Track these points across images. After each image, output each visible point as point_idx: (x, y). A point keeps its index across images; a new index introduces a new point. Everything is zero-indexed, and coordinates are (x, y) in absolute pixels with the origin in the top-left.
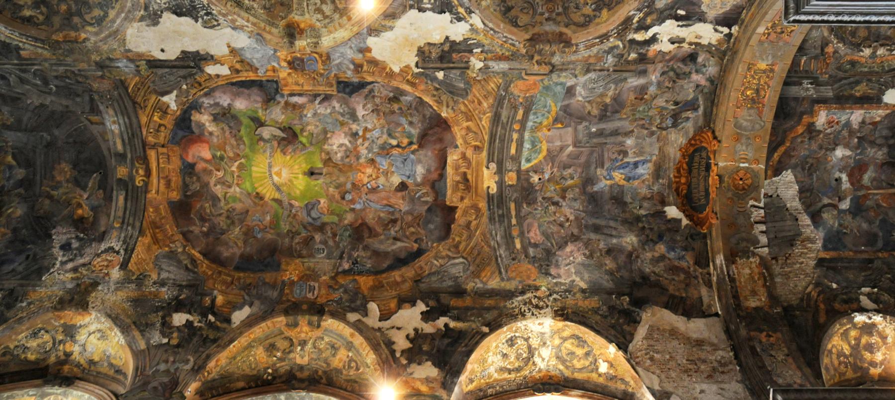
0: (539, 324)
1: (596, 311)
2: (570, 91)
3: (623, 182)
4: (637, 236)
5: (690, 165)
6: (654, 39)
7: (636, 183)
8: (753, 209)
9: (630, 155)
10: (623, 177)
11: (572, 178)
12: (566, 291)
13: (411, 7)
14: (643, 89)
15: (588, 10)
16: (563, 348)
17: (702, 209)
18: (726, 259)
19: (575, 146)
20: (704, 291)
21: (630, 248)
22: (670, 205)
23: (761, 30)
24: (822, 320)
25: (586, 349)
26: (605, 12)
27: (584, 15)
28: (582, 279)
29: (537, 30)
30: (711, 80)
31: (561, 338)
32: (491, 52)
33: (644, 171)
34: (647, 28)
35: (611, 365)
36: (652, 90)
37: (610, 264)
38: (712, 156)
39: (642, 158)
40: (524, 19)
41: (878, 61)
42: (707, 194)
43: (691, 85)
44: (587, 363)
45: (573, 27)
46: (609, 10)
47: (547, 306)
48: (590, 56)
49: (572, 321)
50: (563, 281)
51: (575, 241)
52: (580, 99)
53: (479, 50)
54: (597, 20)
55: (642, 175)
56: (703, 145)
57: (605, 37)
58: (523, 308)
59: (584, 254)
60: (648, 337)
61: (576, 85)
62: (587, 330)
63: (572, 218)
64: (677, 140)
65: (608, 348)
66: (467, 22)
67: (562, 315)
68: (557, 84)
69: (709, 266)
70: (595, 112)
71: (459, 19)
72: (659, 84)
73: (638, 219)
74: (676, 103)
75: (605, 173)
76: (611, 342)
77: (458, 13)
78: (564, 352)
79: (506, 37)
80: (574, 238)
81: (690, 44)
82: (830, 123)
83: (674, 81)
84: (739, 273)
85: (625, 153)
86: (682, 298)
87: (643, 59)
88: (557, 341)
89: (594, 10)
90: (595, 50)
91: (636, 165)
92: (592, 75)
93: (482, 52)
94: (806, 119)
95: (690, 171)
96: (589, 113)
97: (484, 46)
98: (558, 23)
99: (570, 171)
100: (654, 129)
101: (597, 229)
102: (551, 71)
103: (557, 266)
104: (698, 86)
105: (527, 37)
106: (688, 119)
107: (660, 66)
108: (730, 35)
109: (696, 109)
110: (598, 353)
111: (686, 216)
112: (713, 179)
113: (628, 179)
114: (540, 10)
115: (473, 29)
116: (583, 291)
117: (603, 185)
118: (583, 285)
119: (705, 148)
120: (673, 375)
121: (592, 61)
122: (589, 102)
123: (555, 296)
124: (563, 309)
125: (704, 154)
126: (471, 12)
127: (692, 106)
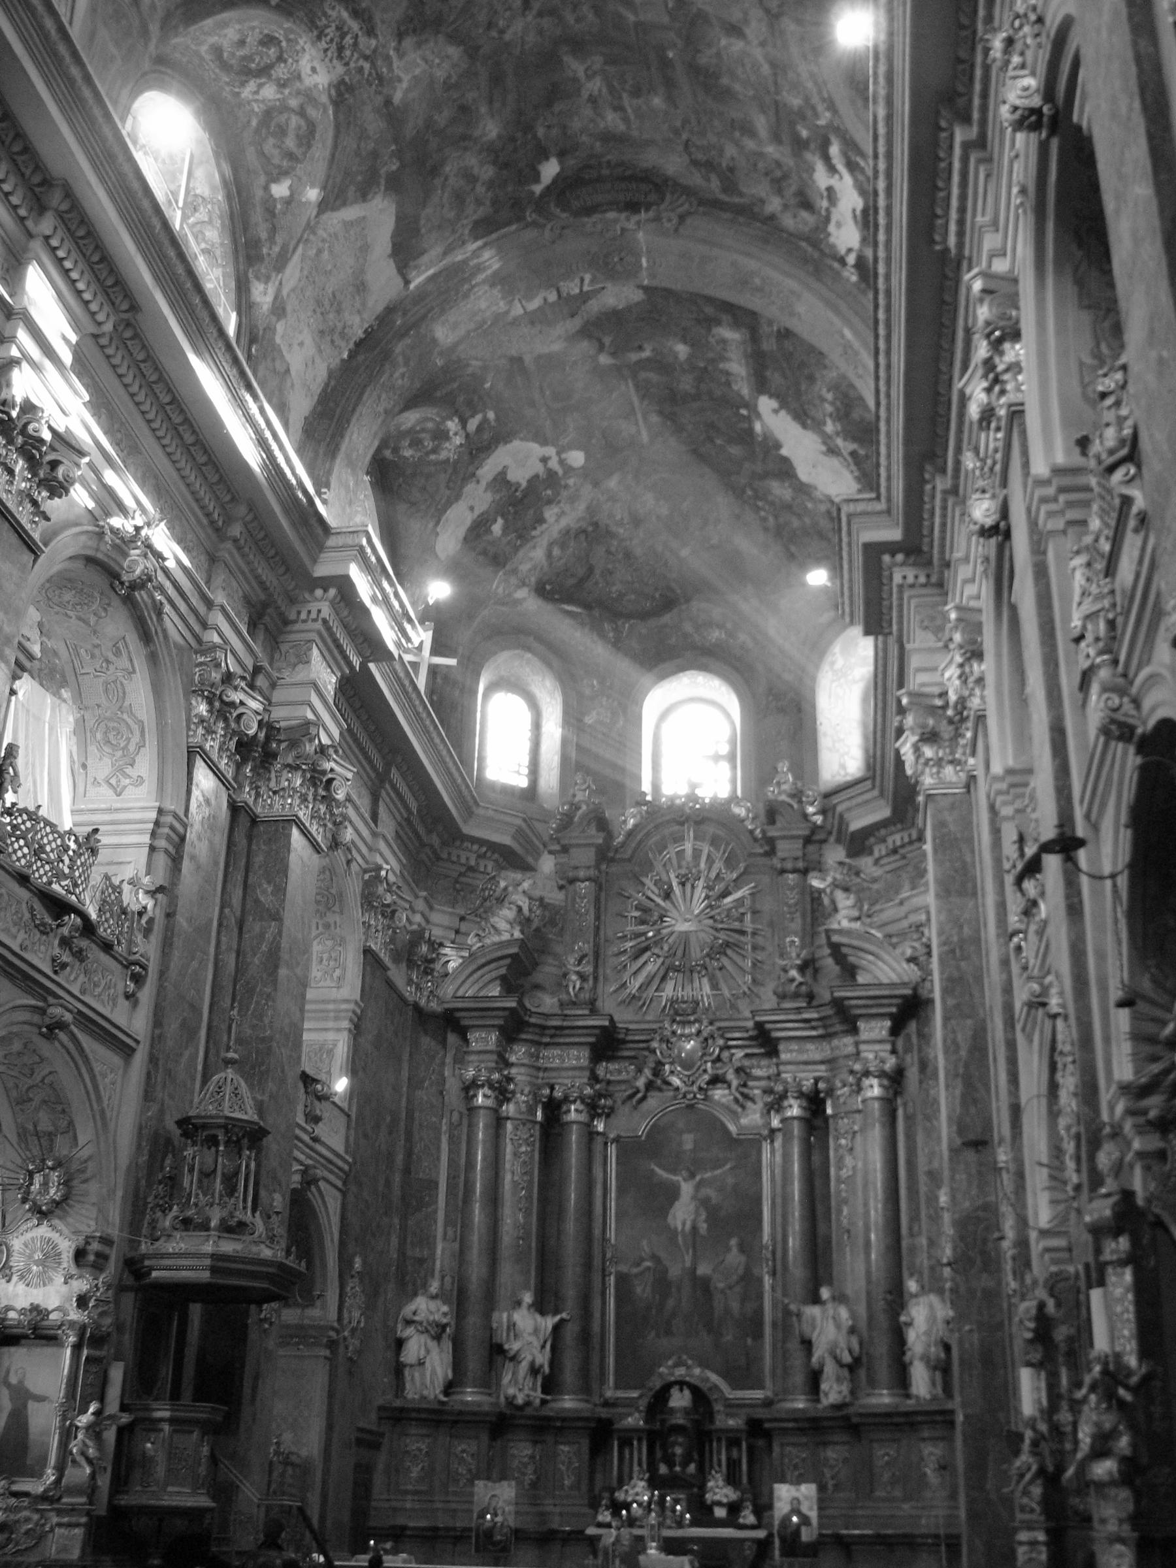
0: (314, 70)
1: (363, 136)
2: (735, 30)
3: (585, 94)
4: (499, 137)
5: (632, 178)
6: (832, 169)
7: (588, 112)
8: (577, 281)
9: (635, 101)
10: (596, 93)
11: (578, 20)
12: (380, 78)
14: (751, 132)
16: (286, 116)
17: (565, 206)
18: (495, 274)
19: (638, 24)
20: (438, 250)
21: (477, 133)
22: (561, 163)
23: (848, 333)
24: (438, 394)
25: (298, 152)
28: (408, 90)
30: (772, 217)
31: (302, 107)
33: (611, 120)
34: (852, 166)
35: (288, 201)
36: (750, 144)
37: (442, 118)
38: (651, 214)
39: (632, 117)
41: (817, 402)
42: (589, 211)
43: (763, 195)
44: (276, 161)
47: (347, 64)
48: (798, 75)
49: (336, 113)
50: (395, 66)
51: (471, 57)
52: (723, 42)
55: (603, 118)
56: (668, 197)
57: (832, 107)
58: (331, 31)
59: (449, 77)
60: (348, 225)
61: (748, 43)
62: (329, 142)
63: (507, 37)
64: (673, 164)
65: (312, 186)
67: (340, 94)
68: (746, 13)
69: (476, 239)
70: (703, 60)
72: (761, 155)
73: (528, 128)
74: (731, 170)
75: (597, 67)
76: (324, 188)
78: (283, 118)
80: (472, 52)
81: (828, 210)
82: (724, 341)
83: (767, 174)
84: (479, 298)
85: (636, 92)
86: (418, 230)
87: (800, 145)
88: (294, 103)
90: (810, 85)
91: (619, 108)
92: (766, 69)
94: (726, 318)
95: (623, 179)
96: (699, 51)
99: (591, 16)
100: (685, 136)
101: (497, 79)
102: (767, 11)
103: (419, 45)
104: (762, 201)
106: (708, 180)
107: (789, 162)
108: (842, 261)
109: (725, 190)
110: (298, 172)
111: (548, 188)
112: (616, 221)
113: (593, 100)
116: (388, 102)
117: (575, 67)
118: (398, 97)
119: (663, 200)
120: (308, 294)
121: (791, 75)
122: (718, 55)
123: (367, 66)
124: (350, 89)
125: (653, 197)
127: (730, 186)
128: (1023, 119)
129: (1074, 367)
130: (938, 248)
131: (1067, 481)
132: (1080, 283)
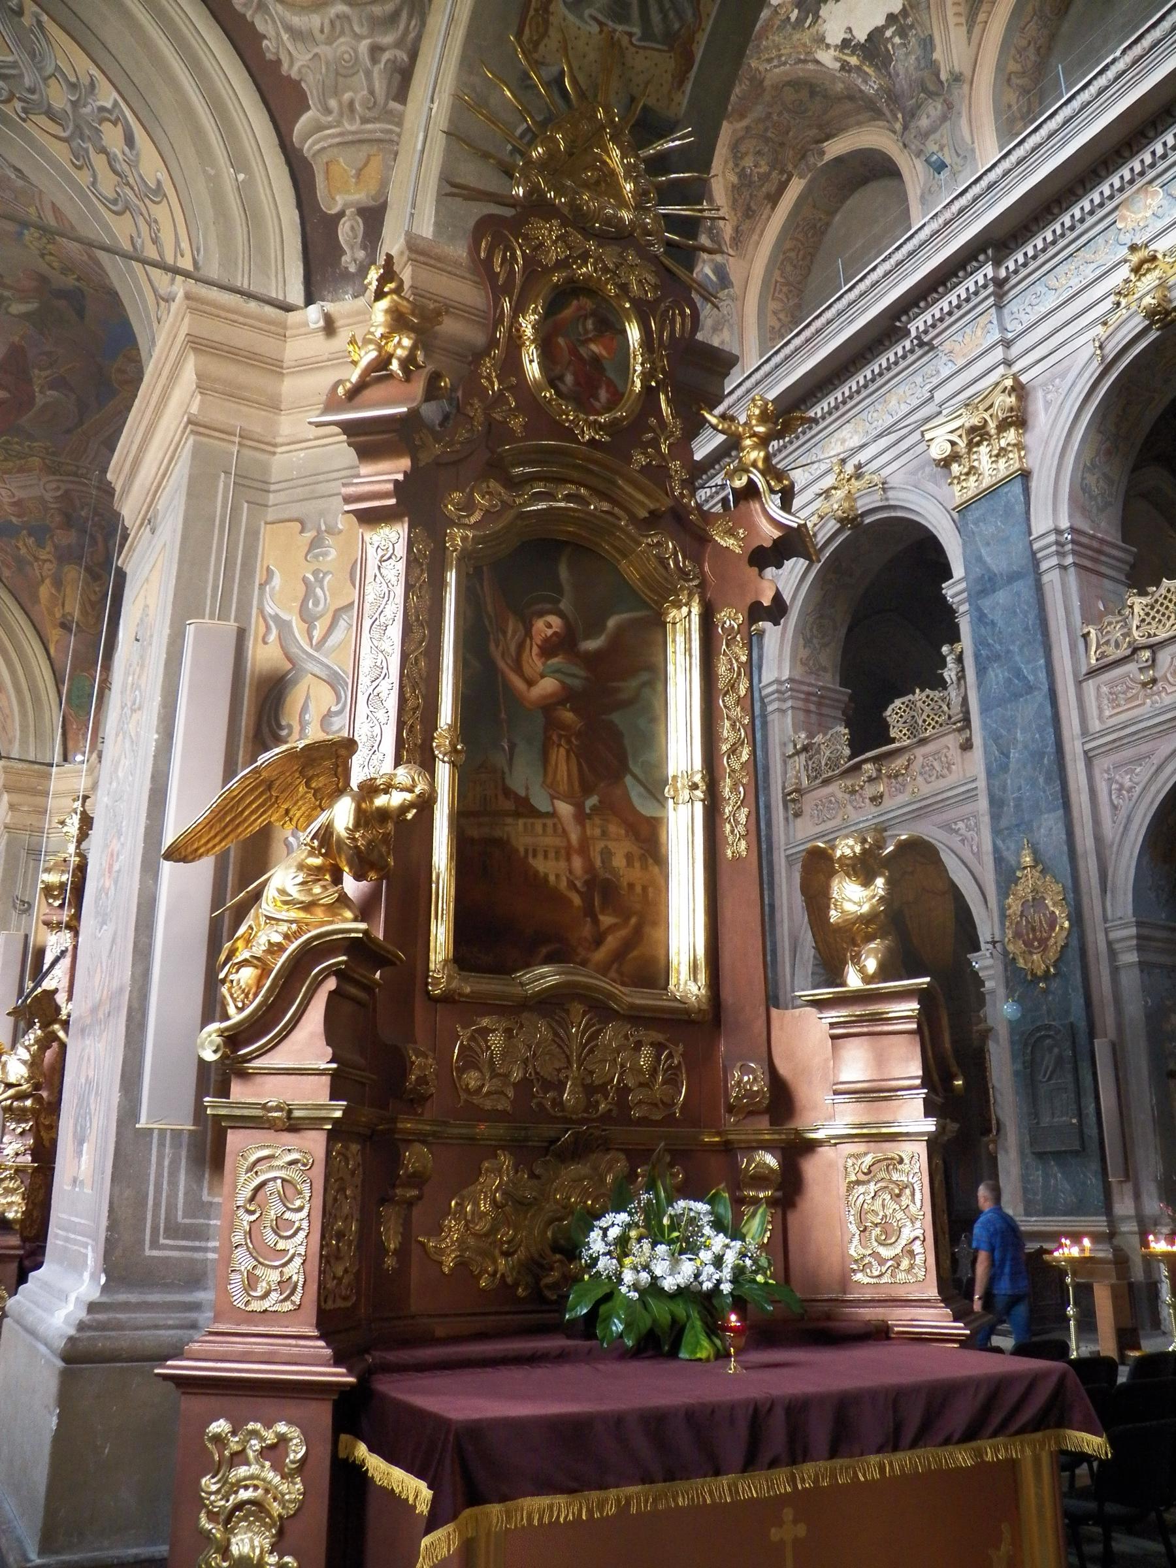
13: (904, 12)
15: (748, 162)
26: (734, 179)
27: (746, 154)
29: (767, 97)
32: (781, 28)
40: (789, 95)
45: (741, 134)
46: (733, 186)
53: (794, 16)
54: (731, 164)
66: (837, 46)
71: (846, 43)
77: (853, 53)
79: (785, 64)
89: (744, 168)
93: (789, 18)
97: (794, 28)
98: (759, 120)
105: (767, 83)
114: (786, 115)
115: (820, 40)
126: (842, 68)
128: (1159, 313)
129: (1081, 466)
130: (898, 324)
131: (1076, 537)
132: (1104, 416)
